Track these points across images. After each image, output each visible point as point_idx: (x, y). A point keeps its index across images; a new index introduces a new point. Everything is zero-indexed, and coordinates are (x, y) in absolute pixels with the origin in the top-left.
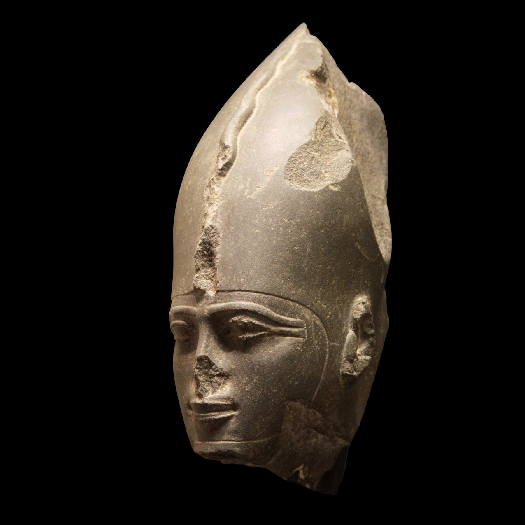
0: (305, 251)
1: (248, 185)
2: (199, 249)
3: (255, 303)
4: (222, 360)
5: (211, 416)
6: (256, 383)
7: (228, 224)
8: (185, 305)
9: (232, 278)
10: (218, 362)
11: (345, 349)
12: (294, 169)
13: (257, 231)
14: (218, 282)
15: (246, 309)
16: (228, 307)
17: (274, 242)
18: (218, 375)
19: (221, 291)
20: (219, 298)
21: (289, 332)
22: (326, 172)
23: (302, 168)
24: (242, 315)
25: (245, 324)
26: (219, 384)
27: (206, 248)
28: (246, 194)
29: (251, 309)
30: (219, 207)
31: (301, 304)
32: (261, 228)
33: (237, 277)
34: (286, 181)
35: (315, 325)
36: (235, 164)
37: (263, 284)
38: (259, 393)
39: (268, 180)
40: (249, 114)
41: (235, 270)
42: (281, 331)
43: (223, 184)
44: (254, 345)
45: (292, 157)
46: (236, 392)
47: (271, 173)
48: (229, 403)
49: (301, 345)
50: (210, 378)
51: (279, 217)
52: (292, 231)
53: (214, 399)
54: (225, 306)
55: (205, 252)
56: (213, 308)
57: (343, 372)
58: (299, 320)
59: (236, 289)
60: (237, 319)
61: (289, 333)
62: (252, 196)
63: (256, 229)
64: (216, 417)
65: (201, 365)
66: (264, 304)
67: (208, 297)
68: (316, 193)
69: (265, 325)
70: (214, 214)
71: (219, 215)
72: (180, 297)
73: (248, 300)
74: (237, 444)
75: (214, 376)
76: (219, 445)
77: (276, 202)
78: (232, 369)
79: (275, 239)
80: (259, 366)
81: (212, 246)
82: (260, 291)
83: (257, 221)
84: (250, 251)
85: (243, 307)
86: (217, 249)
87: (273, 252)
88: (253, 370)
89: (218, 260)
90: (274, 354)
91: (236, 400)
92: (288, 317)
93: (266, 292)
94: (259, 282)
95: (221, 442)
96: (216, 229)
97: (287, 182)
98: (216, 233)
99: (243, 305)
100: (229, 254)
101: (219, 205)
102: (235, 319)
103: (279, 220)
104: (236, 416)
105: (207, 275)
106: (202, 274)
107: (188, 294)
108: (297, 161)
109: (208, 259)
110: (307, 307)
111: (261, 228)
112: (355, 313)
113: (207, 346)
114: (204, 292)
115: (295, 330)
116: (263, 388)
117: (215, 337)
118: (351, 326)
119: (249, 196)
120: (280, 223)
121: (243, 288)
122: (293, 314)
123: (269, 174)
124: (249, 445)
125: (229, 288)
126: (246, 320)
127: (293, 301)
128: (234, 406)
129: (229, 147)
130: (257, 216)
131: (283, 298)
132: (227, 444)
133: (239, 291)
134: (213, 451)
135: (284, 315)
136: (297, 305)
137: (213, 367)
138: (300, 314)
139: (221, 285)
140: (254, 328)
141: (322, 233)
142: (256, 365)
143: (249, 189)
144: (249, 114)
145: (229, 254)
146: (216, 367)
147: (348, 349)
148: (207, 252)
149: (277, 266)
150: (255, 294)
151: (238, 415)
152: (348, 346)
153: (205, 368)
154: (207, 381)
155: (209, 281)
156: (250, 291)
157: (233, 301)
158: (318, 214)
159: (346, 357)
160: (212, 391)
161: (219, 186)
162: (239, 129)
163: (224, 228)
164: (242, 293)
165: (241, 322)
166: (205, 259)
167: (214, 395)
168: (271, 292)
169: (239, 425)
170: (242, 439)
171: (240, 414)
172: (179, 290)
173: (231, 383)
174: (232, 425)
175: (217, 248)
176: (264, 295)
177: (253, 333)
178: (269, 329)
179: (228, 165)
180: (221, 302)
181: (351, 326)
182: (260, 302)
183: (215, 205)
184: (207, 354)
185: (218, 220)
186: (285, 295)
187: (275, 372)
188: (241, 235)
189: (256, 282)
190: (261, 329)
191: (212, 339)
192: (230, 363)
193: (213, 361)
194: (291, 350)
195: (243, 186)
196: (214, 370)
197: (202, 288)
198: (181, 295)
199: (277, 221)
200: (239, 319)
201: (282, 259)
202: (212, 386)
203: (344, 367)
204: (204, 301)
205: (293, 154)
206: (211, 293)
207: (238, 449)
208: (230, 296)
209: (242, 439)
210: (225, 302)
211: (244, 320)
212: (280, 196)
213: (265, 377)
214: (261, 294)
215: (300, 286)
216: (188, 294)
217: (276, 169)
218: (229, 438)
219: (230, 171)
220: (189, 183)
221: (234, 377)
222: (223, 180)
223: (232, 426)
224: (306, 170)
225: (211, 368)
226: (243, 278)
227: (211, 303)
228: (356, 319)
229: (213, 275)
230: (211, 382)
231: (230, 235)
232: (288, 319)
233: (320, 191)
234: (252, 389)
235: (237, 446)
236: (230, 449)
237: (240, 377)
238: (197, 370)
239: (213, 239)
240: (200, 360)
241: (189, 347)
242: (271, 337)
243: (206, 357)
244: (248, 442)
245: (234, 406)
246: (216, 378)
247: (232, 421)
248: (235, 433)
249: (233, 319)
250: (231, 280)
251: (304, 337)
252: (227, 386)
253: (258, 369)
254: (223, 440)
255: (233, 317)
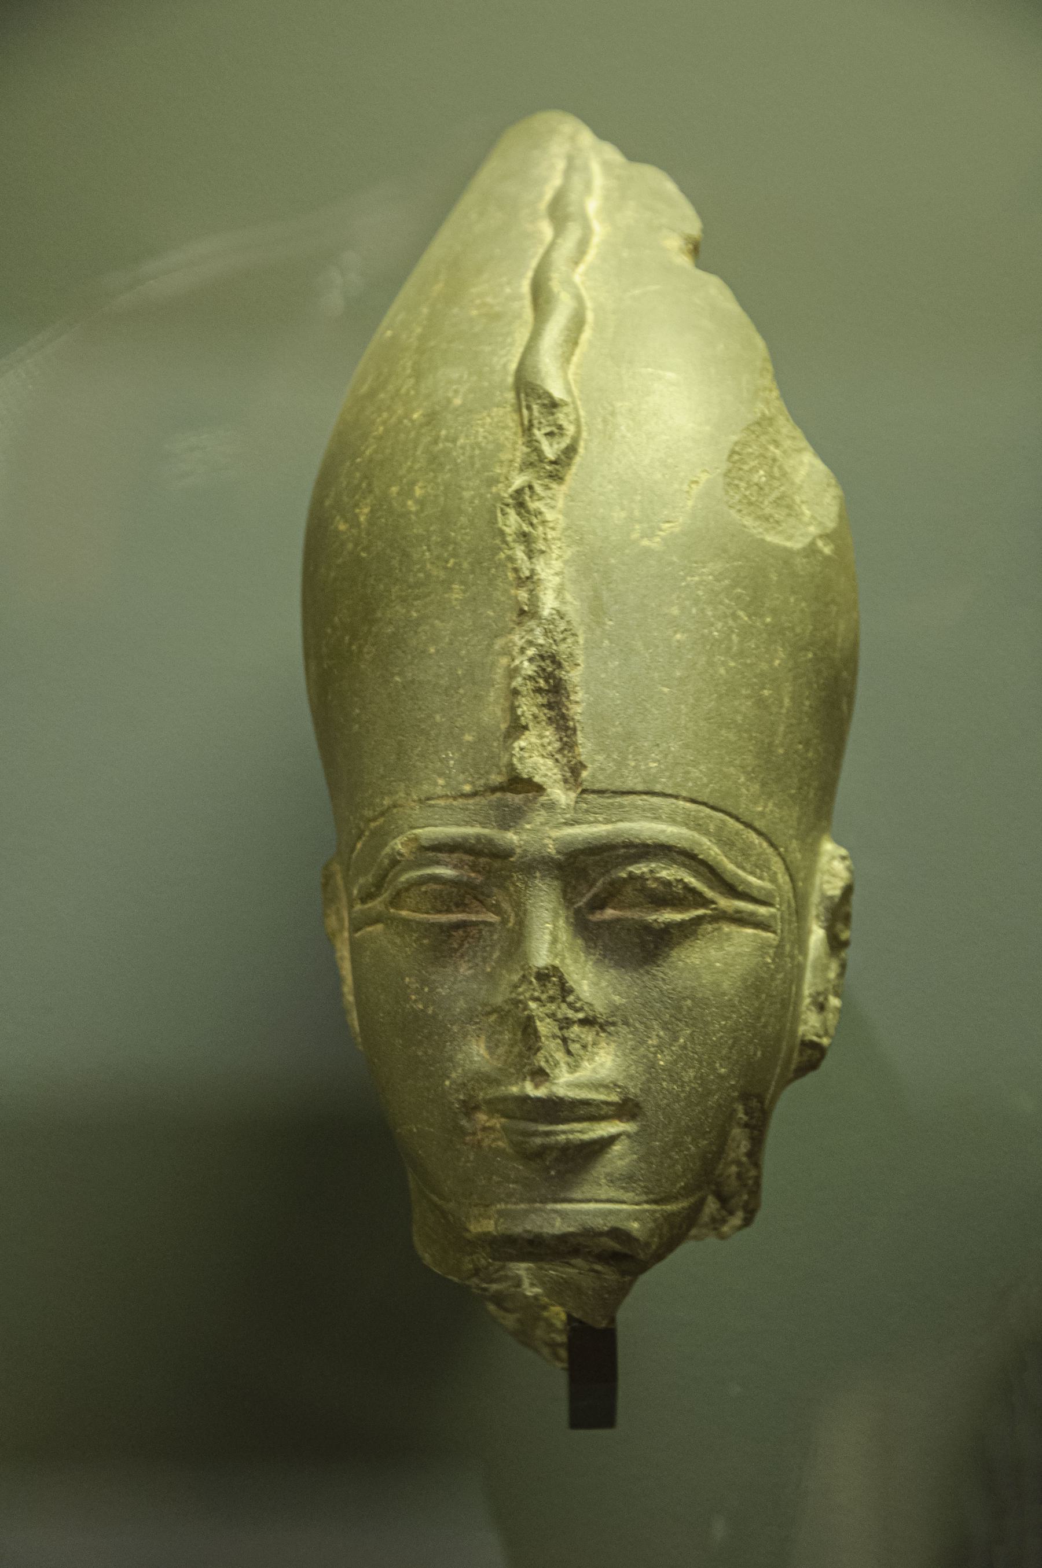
0: (781, 702)
1: (637, 513)
2: (530, 673)
3: (689, 828)
4: (591, 983)
5: (572, 1132)
6: (684, 1047)
7: (596, 610)
8: (467, 823)
9: (626, 759)
10: (580, 985)
11: (808, 976)
12: (743, 484)
13: (678, 636)
14: (584, 767)
15: (671, 843)
16: (618, 836)
17: (722, 671)
18: (583, 1022)
19: (594, 792)
20: (587, 811)
21: (752, 914)
22: (803, 502)
23: (757, 484)
24: (659, 861)
25: (668, 884)
26: (584, 1047)
27: (544, 670)
28: (635, 536)
29: (683, 844)
30: (566, 562)
31: (772, 844)
32: (688, 631)
33: (640, 757)
34: (733, 512)
35: (789, 902)
36: (581, 450)
37: (705, 780)
38: (692, 1073)
39: (690, 503)
40: (577, 323)
41: (629, 736)
42: (738, 911)
43: (560, 503)
44: (679, 943)
45: (733, 452)
46: (632, 1071)
47: (693, 486)
48: (614, 1098)
49: (771, 951)
50: (561, 1029)
51: (728, 607)
52: (757, 647)
53: (579, 1085)
54: (608, 832)
55: (542, 683)
56: (575, 837)
57: (804, 1035)
58: (767, 885)
59: (640, 787)
60: (645, 870)
61: (753, 919)
62: (654, 543)
63: (676, 632)
64: (585, 1137)
65: (543, 992)
66: (707, 833)
67: (551, 806)
68: (798, 552)
69: (709, 893)
70: (557, 580)
71: (569, 586)
72: (442, 802)
73: (673, 821)
74: (635, 1211)
75: (574, 1022)
76: (587, 1213)
77: (718, 566)
78: (617, 1008)
79: (724, 663)
80: (693, 1000)
81: (559, 666)
82: (700, 799)
83: (675, 611)
84: (666, 690)
85: (663, 839)
86: (574, 676)
87: (720, 697)
88: (680, 1011)
89: (578, 709)
90: (725, 972)
91: (633, 1090)
92: (752, 873)
93: (711, 803)
94: (695, 773)
95: (592, 1206)
96: (568, 622)
97: (737, 516)
98: (570, 632)
99: (663, 832)
100: (612, 693)
101: (566, 557)
102: (640, 869)
103: (729, 612)
104: (629, 1135)
105: (543, 746)
106: (533, 740)
107: (474, 794)
108: (745, 463)
109: (545, 701)
110: (779, 854)
111: (688, 631)
112: (828, 882)
113: (555, 941)
114: (540, 789)
115: (763, 910)
116: (700, 1062)
117: (567, 918)
118: (818, 917)
119: (645, 542)
120: (731, 623)
121: (658, 788)
122: (761, 867)
123: (685, 487)
124: (658, 1215)
125: (618, 785)
126: (668, 873)
127: (760, 833)
128: (627, 1109)
129: (566, 404)
130: (674, 596)
131: (743, 823)
132: (611, 1212)
133: (646, 793)
134: (571, 1229)
135: (743, 869)
136: (765, 845)
137: (571, 998)
138: (769, 869)
139: (593, 776)
140: (691, 898)
141: (810, 660)
142: (684, 999)
143: (640, 522)
144: (577, 323)
145: (612, 693)
146: (579, 999)
147: (814, 977)
148: (546, 681)
149: (732, 737)
150: (688, 805)
151: (636, 1134)
152: (815, 968)
153: (552, 999)
154: (555, 1036)
155: (550, 763)
156: (676, 797)
157: (631, 820)
158: (802, 611)
159: (811, 995)
160: (568, 1064)
161: (553, 507)
162: (566, 359)
163: (587, 620)
164: (655, 800)
165: (657, 879)
166: (541, 700)
167: (577, 1075)
168: (721, 804)
169: (639, 1160)
170: (644, 1198)
171: (643, 1129)
172: (436, 784)
173: (613, 1045)
174: (619, 1157)
175: (572, 674)
176: (708, 811)
177: (680, 912)
178: (713, 902)
179: (570, 451)
180: (597, 822)
181: (818, 917)
182: (699, 826)
183: (554, 556)
184: (557, 962)
185: (568, 597)
186: (747, 819)
187: (726, 1018)
188: (639, 645)
189: (688, 772)
190: (698, 899)
191: (561, 923)
192: (610, 990)
193: (571, 983)
194: (757, 964)
195: (623, 514)
196: (571, 1006)
197: (537, 779)
198: (447, 796)
199: (726, 616)
200: (651, 871)
201: (739, 718)
202: (569, 1053)
203: (806, 1023)
204: (540, 817)
205: (736, 443)
206: (561, 795)
207: (636, 1225)
208: (621, 806)
209: (644, 1198)
210: (608, 821)
211: (664, 874)
212: (725, 551)
213: (707, 1034)
214: (701, 807)
215: (770, 796)
216: (474, 794)
217: (704, 477)
218: (613, 1194)
219: (574, 469)
220: (418, 492)
221: (623, 1030)
222: (560, 491)
223: (620, 1163)
224: (767, 490)
225: (564, 1001)
226: (654, 761)
227: (566, 824)
228: (831, 898)
229: (558, 745)
230: (565, 1040)
231: (606, 642)
232: (751, 879)
233: (804, 549)
234: (676, 1062)
235: (636, 1216)
236: (619, 1225)
237: (641, 1027)
238: (533, 1005)
239: (563, 647)
240: (543, 976)
241: (461, 945)
242: (716, 926)
243: (555, 968)
244: (654, 1207)
245: (627, 1109)
246: (576, 1028)
247: (617, 1148)
248: (627, 1180)
249: (630, 869)
250: (621, 764)
251: (774, 932)
252: (602, 1052)
253: (690, 1009)
254: (597, 1201)
255: (631, 864)
